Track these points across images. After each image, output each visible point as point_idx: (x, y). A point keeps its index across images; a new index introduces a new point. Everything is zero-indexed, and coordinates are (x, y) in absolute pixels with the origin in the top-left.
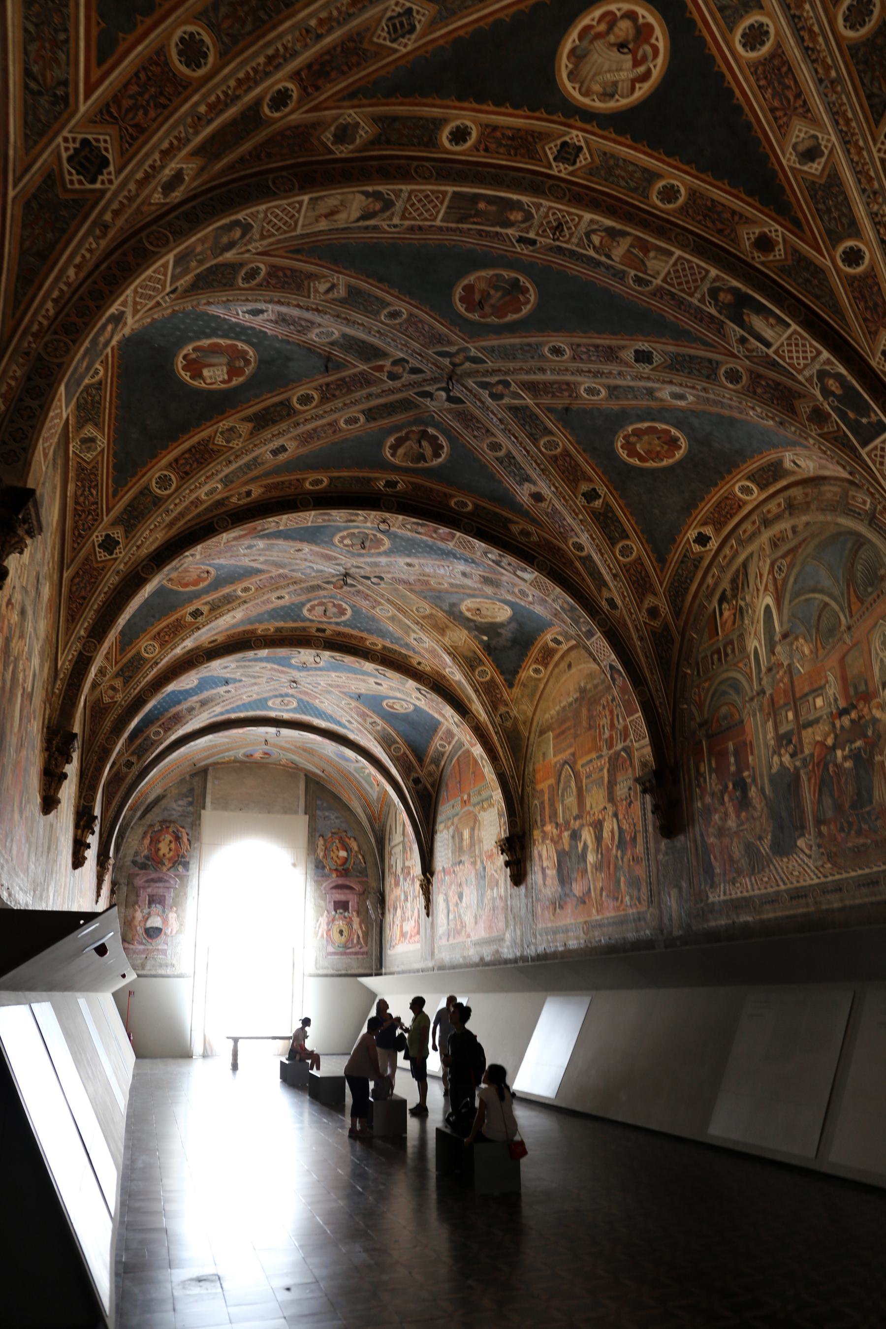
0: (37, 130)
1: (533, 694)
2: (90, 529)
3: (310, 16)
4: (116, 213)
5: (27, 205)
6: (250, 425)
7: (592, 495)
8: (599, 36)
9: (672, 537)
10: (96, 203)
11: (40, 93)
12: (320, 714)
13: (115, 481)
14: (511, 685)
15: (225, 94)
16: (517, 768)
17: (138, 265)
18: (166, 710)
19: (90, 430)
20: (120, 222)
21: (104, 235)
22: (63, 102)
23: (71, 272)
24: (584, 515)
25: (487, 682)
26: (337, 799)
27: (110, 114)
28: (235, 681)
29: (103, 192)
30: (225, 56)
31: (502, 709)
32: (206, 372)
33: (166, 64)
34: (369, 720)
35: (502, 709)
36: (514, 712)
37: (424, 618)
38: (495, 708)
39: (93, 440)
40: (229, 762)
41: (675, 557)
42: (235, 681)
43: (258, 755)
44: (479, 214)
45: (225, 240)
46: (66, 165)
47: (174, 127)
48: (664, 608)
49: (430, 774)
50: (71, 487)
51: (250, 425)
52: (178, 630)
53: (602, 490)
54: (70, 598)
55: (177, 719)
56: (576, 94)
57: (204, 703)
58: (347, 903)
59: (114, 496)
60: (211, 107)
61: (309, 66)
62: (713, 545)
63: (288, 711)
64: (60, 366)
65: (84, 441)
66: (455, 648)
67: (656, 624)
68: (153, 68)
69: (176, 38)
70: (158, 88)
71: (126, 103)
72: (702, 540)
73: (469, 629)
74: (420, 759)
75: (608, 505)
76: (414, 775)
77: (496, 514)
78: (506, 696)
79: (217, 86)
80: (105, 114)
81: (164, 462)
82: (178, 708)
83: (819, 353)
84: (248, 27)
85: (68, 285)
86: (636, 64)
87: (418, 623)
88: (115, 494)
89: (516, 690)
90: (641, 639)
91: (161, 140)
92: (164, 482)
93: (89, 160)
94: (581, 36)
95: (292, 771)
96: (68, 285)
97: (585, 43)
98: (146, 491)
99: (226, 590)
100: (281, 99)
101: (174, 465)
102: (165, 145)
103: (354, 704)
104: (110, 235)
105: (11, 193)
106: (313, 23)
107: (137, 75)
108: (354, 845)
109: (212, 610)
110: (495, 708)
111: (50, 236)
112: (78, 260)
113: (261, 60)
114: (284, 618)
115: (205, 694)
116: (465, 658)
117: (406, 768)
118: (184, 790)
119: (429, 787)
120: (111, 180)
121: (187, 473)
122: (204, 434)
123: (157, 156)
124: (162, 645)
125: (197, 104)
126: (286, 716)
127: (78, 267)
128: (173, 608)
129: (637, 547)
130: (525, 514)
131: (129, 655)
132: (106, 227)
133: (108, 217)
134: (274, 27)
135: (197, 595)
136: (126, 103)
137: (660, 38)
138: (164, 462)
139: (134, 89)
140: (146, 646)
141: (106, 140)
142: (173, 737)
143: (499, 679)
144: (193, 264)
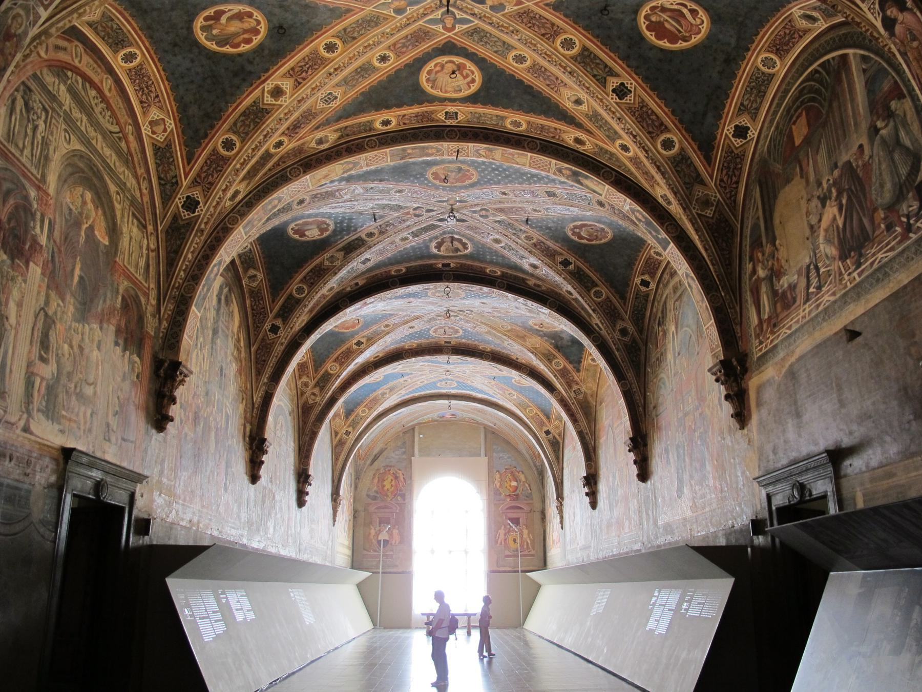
0: (167, 199)
1: (594, 375)
2: (263, 322)
3: (280, 114)
4: (206, 223)
5: (167, 232)
6: (342, 253)
7: (566, 263)
8: (437, 72)
9: (626, 282)
12: (475, 389)
13: (272, 294)
14: (578, 371)
16: (590, 427)
17: (224, 237)
18: (368, 395)
19: (252, 272)
20: (208, 227)
21: (202, 234)
22: (176, 184)
23: (190, 256)
24: (565, 274)
25: (561, 370)
26: (508, 443)
28: (408, 374)
29: (199, 216)
30: (244, 142)
31: (575, 387)
32: (307, 233)
34: (507, 392)
35: (575, 387)
36: (583, 389)
37: (508, 331)
38: (570, 387)
39: (255, 276)
40: (429, 422)
41: (631, 296)
42: (408, 374)
43: (448, 416)
44: (409, 154)
46: (181, 210)
47: (227, 177)
48: (631, 328)
49: (557, 427)
50: (248, 302)
51: (342, 253)
52: (348, 355)
53: (572, 259)
54: (256, 362)
55: (376, 401)
56: (440, 93)
57: (392, 390)
58: (519, 519)
59: (273, 302)
60: (242, 164)
61: (288, 129)
62: (653, 286)
63: (453, 388)
64: (191, 297)
65: (250, 278)
66: (535, 349)
67: (626, 339)
69: (220, 142)
70: (218, 163)
71: (203, 175)
72: (645, 283)
73: (540, 336)
74: (548, 418)
75: (578, 267)
76: (545, 429)
77: (516, 276)
78: (576, 378)
80: (195, 183)
81: (298, 279)
82: (375, 394)
83: (625, 201)
84: (252, 126)
85: (189, 261)
86: (465, 77)
87: (505, 335)
88: (273, 302)
89: (583, 374)
90: (618, 350)
91: (222, 185)
92: (300, 290)
93: (191, 205)
94: (436, 65)
95: (473, 425)
96: (189, 261)
97: (433, 75)
98: (291, 296)
99: (374, 328)
100: (279, 144)
101: (304, 280)
102: (224, 187)
103: (493, 382)
104: (205, 233)
105: (160, 229)
106: (282, 116)
107: (206, 162)
108: (522, 477)
109: (368, 340)
110: (570, 387)
111: (178, 242)
112: (192, 249)
113: (261, 137)
114: (419, 338)
115: (391, 384)
116: (544, 354)
117: (542, 424)
118: (399, 444)
119: (557, 436)
121: (312, 284)
122: (317, 261)
123: (221, 193)
124: (341, 364)
126: (454, 392)
127: (193, 252)
128: (343, 342)
129: (605, 291)
130: (532, 275)
131: (321, 373)
132: (202, 231)
133: (203, 226)
134: (264, 123)
135: (357, 333)
136: (203, 175)
137: (470, 65)
138: (298, 279)
139: (205, 168)
140: (330, 366)
141: (197, 194)
142: (376, 413)
143: (570, 367)
144: (256, 223)
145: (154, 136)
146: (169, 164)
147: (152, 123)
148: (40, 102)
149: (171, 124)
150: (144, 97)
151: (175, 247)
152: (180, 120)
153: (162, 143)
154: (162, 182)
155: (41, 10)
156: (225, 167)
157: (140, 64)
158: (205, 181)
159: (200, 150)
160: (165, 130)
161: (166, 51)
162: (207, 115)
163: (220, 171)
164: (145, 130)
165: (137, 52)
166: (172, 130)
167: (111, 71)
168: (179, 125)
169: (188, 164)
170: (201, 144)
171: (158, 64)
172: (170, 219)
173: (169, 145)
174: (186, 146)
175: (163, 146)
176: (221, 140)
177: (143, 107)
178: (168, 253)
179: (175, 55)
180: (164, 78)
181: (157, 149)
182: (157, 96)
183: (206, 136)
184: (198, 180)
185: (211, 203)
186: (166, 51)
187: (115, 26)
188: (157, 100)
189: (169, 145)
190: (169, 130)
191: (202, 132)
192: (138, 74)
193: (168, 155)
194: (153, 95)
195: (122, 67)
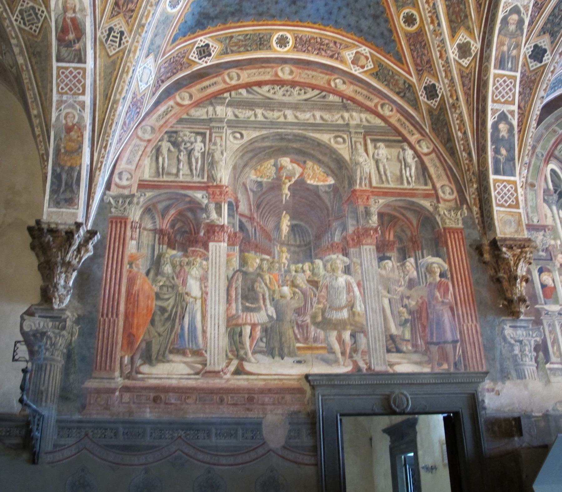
5: (433, 129)
10: (444, 101)
11: (405, 94)
15: (429, 12)
22: (410, 87)
27: (420, 71)
29: (443, 95)
33: (411, 34)
45: (512, 28)
46: (429, 102)
68: (411, 41)
69: (403, 25)
71: (418, 61)
79: (425, 15)
80: (420, 73)
85: (462, 139)
93: (431, 91)
102: (438, 54)
107: (411, 50)
120: (442, 88)
125: (429, 29)
136: (418, 61)
141: (428, 80)
145: (366, 69)
146: (392, 77)
147: (355, 62)
148: (191, 132)
149: (365, 50)
150: (328, 52)
151: (446, 136)
152: (366, 40)
153: (374, 67)
154: (402, 94)
155: (81, 98)
156: (425, 38)
157: (296, 38)
158: (424, 66)
159: (398, 45)
160: (367, 58)
161: (296, 13)
162: (375, 17)
163: (425, 45)
164: (356, 71)
165: (281, 33)
166: (370, 53)
167: (285, 61)
168: (369, 45)
169: (403, 64)
170: (394, 41)
171: (306, 24)
172: (428, 117)
173: (379, 64)
174: (389, 53)
175: (377, 69)
176: (402, 23)
177: (337, 59)
178: (445, 145)
179: (304, 8)
180: (321, 27)
181: (376, 75)
182: (335, 43)
183: (390, 31)
184: (420, 68)
185: (442, 77)
186: (296, 13)
187: (240, 37)
188: (338, 45)
189: (379, 64)
190: (368, 55)
191: (386, 33)
192: (302, 44)
193: (386, 72)
194: (332, 45)
195: (288, 51)
